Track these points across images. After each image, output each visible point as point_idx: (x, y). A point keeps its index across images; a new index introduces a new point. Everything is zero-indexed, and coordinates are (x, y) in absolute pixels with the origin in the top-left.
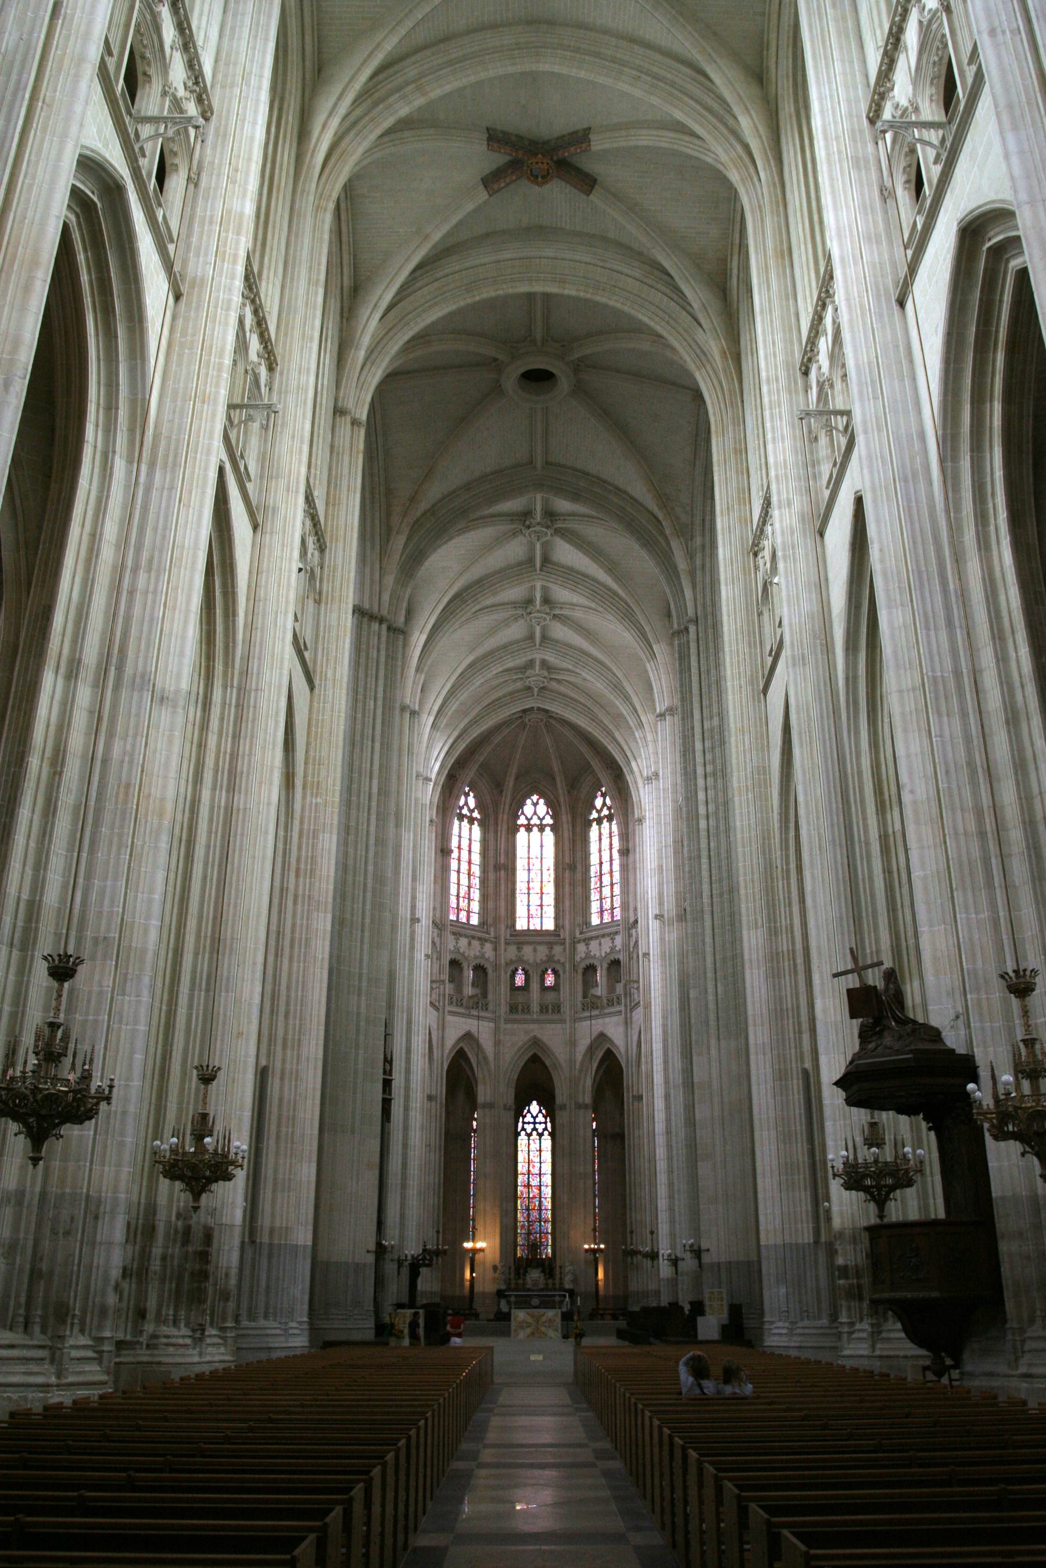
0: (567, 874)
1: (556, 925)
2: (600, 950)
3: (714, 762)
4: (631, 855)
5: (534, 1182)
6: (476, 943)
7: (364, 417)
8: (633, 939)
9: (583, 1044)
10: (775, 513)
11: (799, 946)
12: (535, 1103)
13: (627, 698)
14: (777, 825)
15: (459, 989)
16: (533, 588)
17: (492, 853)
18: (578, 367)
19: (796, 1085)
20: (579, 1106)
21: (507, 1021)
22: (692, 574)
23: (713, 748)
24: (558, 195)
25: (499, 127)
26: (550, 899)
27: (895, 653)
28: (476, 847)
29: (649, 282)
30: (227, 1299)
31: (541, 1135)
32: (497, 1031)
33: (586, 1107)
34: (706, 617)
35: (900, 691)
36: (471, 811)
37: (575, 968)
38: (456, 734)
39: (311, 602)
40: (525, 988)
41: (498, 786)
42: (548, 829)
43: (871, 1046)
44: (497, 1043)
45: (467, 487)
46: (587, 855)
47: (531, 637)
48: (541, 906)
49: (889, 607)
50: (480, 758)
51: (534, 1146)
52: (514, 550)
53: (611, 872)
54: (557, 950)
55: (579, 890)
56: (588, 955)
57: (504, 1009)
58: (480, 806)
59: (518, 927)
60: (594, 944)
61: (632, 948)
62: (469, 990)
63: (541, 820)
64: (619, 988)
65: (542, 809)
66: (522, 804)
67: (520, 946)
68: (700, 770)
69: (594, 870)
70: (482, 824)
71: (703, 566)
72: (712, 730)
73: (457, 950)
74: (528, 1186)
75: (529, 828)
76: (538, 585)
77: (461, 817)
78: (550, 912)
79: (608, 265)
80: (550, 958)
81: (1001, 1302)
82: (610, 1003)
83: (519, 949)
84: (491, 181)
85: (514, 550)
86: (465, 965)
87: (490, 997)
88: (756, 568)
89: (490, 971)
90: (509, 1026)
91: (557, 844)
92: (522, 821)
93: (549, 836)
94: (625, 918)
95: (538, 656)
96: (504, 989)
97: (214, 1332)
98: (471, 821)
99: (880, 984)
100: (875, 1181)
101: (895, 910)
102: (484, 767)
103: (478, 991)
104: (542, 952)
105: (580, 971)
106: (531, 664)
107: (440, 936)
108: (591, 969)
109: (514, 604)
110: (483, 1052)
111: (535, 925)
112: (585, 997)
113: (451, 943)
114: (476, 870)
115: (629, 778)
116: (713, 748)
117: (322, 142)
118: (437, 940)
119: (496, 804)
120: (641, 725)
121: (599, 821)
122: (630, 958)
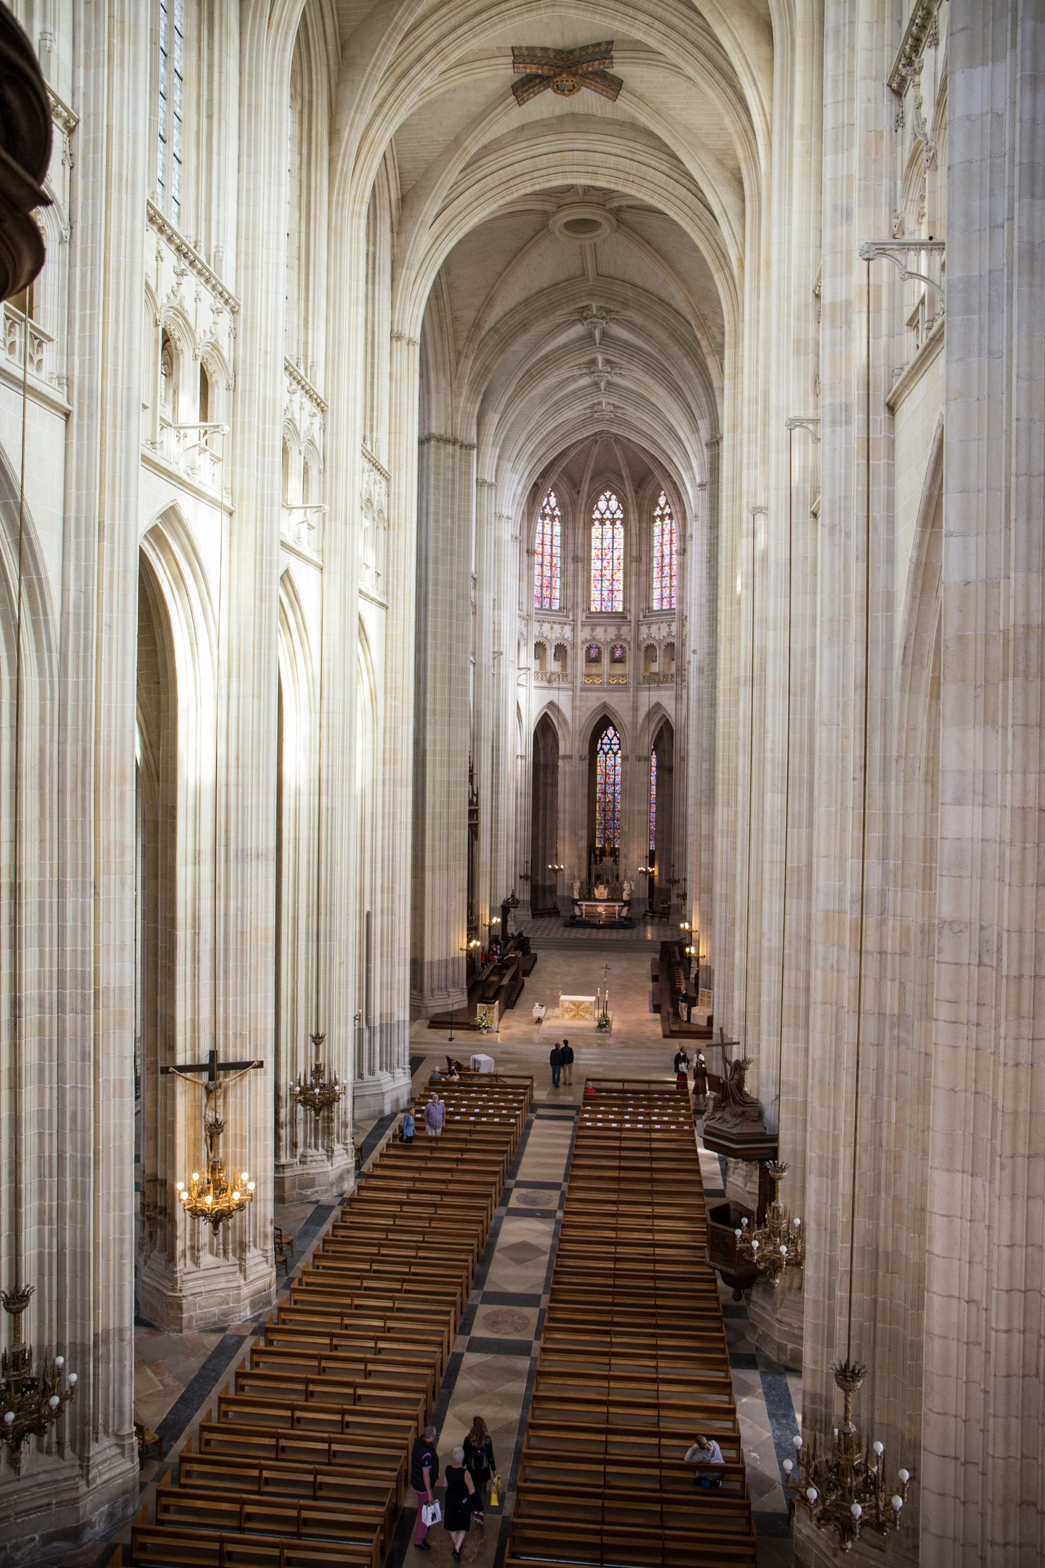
1: (624, 608)
2: (659, 632)
5: (610, 790)
6: (557, 627)
7: (417, 336)
17: (570, 547)
24: (587, 99)
25: (524, 44)
26: (619, 586)
27: (772, 831)
28: (557, 542)
29: (675, 176)
31: (615, 754)
35: (771, 862)
36: (553, 510)
37: (638, 646)
38: (535, 460)
39: (381, 530)
42: (618, 522)
43: (718, 1115)
44: (574, 708)
45: (526, 302)
46: (650, 548)
47: (596, 384)
48: (612, 591)
49: (773, 792)
51: (610, 763)
52: (578, 330)
53: (671, 565)
54: (624, 630)
55: (643, 579)
56: (649, 636)
57: (580, 680)
58: (559, 504)
59: (593, 609)
60: (654, 628)
61: (682, 637)
62: (553, 666)
63: (613, 514)
65: (614, 504)
66: (596, 501)
69: (656, 553)
70: (563, 520)
74: (605, 793)
75: (602, 522)
77: (544, 516)
78: (620, 596)
79: (637, 157)
80: (619, 637)
84: (523, 88)
86: (548, 646)
89: (569, 649)
91: (625, 536)
92: (597, 515)
93: (620, 531)
97: (341, 1146)
98: (553, 518)
102: (566, 473)
104: (612, 632)
105: (643, 649)
107: (527, 625)
110: (563, 716)
111: (607, 607)
112: (646, 670)
114: (557, 561)
117: (350, 138)
118: (524, 630)
119: (574, 503)
121: (662, 518)
122: (683, 645)
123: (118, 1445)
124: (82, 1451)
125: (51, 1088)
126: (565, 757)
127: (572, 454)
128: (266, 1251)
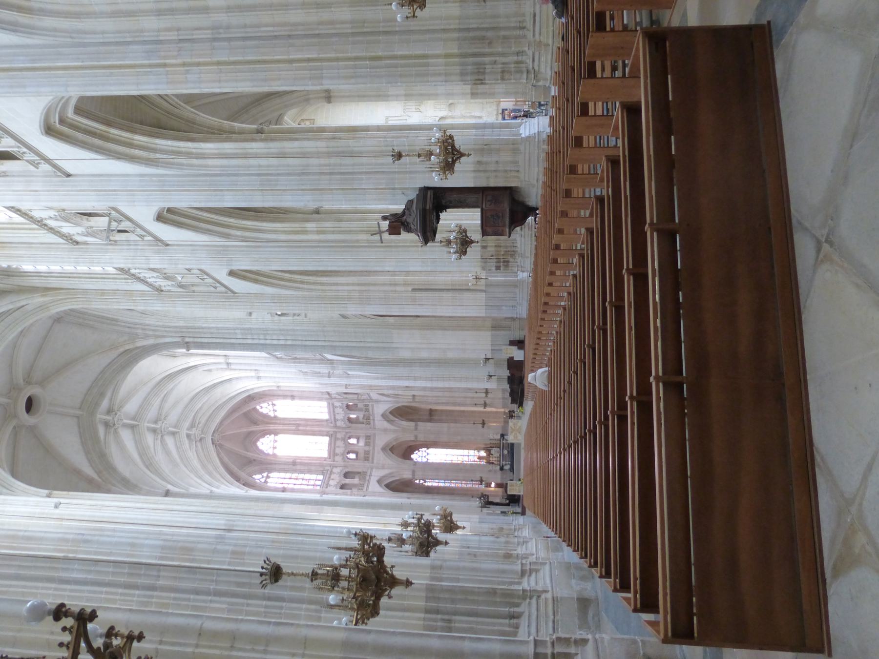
0: (301, 428)
2: (341, 414)
3: (259, 334)
4: (295, 394)
6: (333, 476)
8: (337, 396)
9: (386, 425)
10: (152, 266)
11: (357, 288)
12: (412, 456)
13: (214, 386)
14: (300, 293)
15: (355, 486)
16: (149, 429)
17: (286, 467)
18: (28, 381)
19: (418, 294)
20: (416, 429)
21: (373, 462)
22: (157, 337)
23: (252, 334)
28: (282, 475)
30: (502, 529)
32: (377, 468)
33: (416, 425)
34: (182, 332)
40: (357, 453)
41: (250, 462)
43: (412, 226)
44: (383, 467)
45: (87, 453)
47: (173, 434)
50: (235, 469)
52: (126, 436)
54: (339, 436)
55: (309, 423)
56: (342, 420)
57: (367, 464)
58: (261, 472)
60: (338, 417)
62: (356, 481)
64: (360, 405)
67: (335, 455)
68: (262, 342)
70: (270, 471)
71: (154, 330)
72: (242, 334)
73: (336, 486)
76: (146, 424)
77: (266, 482)
81: (510, 188)
82: (367, 410)
83: (337, 455)
85: (126, 436)
86: (343, 482)
87: (360, 470)
88: (169, 291)
89: (347, 470)
90: (375, 461)
93: (280, 437)
94: (326, 400)
95: (184, 432)
96: (356, 463)
98: (268, 477)
99: (387, 222)
100: (464, 243)
101: (350, 231)
103: (357, 476)
104: (340, 443)
106: (188, 436)
108: (350, 420)
109: (155, 440)
112: (363, 423)
113: (330, 489)
114: (294, 475)
115: (256, 391)
116: (252, 334)
120: (229, 380)
121: (275, 411)
123: (530, 575)
124: (519, 597)
125: (211, 601)
126: (413, 475)
127: (226, 459)
128: (518, 544)
